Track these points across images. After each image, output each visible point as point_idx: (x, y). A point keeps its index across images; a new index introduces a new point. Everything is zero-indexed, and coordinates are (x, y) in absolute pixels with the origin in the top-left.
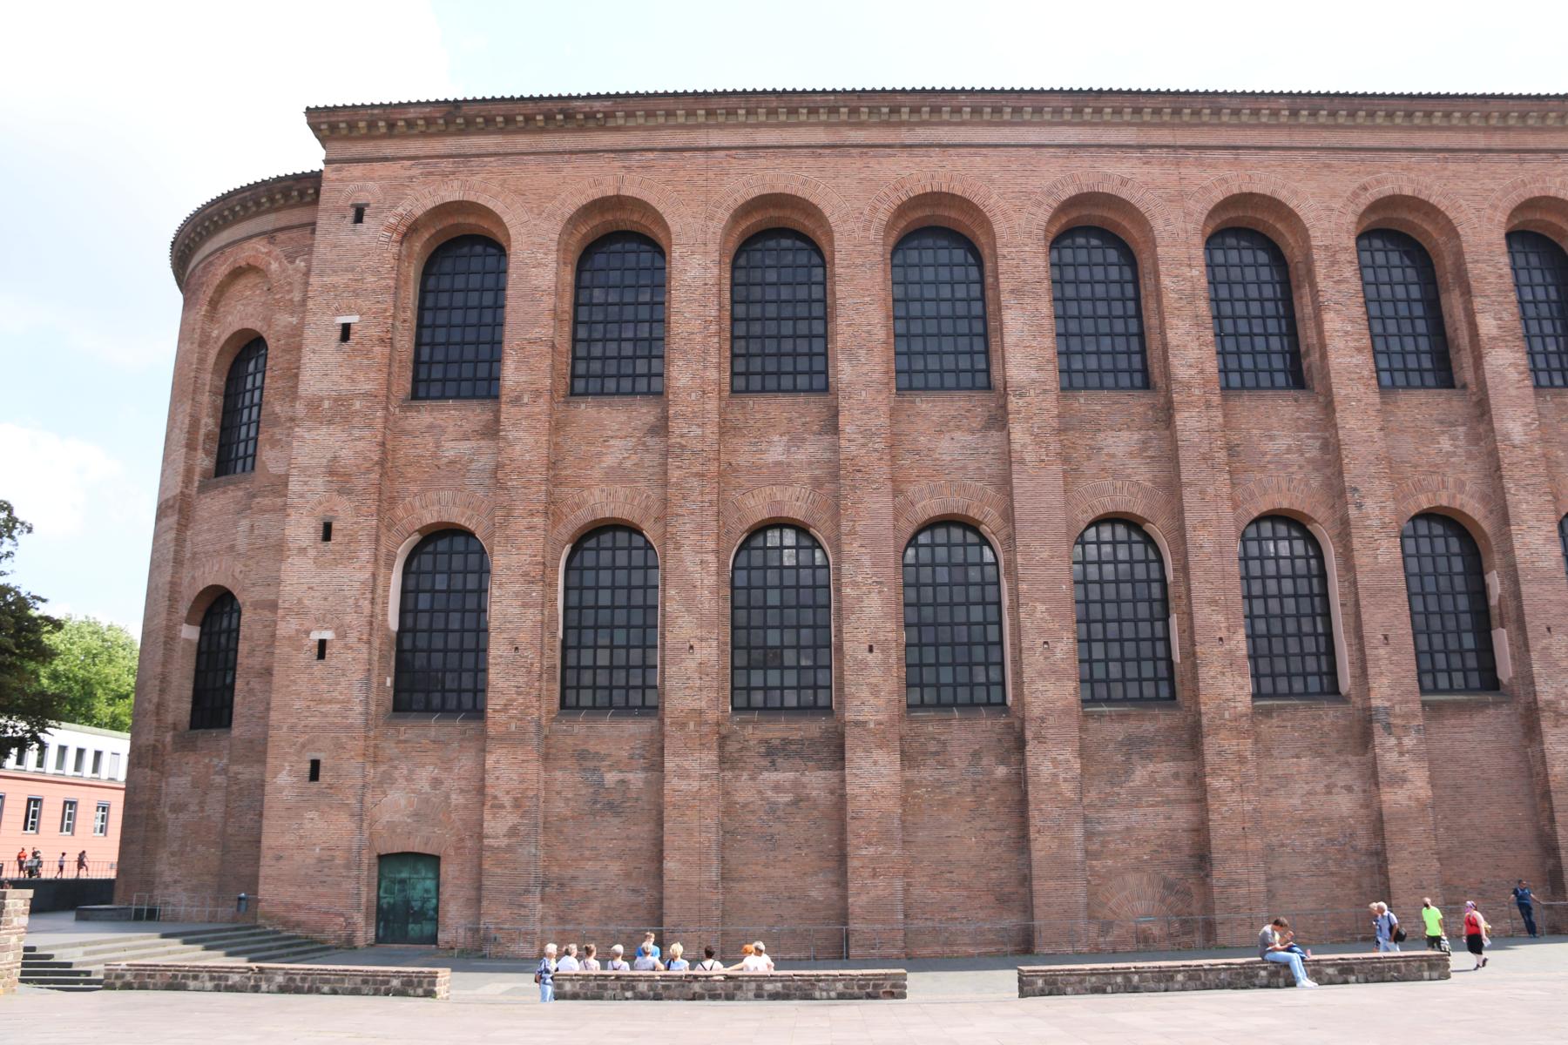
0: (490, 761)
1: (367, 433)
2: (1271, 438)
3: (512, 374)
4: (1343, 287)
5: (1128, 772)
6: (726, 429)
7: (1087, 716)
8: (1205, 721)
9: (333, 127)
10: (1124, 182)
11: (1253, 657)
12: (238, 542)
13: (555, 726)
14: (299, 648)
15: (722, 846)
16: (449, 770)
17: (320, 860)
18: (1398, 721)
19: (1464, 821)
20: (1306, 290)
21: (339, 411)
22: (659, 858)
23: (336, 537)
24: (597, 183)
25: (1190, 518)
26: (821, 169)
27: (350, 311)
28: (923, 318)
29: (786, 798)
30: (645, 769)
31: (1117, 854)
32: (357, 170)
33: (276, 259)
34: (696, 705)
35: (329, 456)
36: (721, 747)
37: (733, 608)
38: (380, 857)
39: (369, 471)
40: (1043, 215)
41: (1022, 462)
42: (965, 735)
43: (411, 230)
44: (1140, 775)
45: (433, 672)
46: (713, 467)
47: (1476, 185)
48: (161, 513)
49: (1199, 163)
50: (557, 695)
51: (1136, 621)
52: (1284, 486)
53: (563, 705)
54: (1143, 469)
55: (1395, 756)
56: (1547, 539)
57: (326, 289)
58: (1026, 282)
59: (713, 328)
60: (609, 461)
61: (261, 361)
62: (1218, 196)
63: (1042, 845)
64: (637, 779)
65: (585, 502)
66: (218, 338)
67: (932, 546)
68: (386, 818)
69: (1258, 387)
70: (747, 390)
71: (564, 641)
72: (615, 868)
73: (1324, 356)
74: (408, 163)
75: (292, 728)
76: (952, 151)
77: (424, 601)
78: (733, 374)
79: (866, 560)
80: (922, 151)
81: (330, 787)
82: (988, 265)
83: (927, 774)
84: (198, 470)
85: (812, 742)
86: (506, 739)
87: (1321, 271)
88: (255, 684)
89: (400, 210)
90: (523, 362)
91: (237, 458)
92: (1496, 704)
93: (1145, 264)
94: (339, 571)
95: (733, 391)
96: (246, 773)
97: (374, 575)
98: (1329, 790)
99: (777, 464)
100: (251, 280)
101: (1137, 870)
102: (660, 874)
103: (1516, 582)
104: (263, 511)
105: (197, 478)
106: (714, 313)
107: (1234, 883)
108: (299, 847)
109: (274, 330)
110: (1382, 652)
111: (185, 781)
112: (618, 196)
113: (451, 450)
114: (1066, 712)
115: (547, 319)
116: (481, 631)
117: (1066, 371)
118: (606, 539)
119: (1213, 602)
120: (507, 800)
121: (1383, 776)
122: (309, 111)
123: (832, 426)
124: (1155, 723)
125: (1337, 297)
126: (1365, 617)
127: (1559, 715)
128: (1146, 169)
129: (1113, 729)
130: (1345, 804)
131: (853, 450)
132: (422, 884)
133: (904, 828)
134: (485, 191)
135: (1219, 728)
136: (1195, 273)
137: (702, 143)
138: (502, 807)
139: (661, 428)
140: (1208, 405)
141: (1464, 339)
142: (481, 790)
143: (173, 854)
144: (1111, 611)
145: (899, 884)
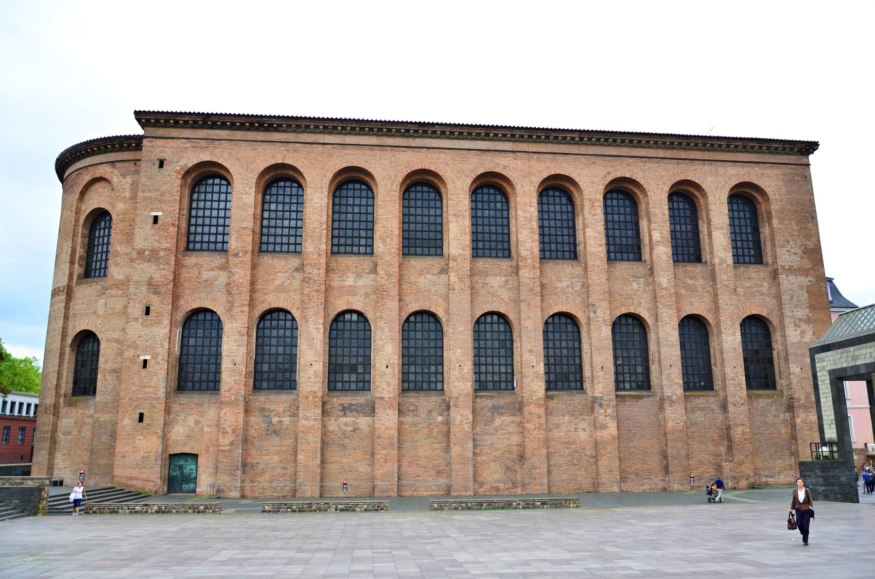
0: (222, 414)
1: (166, 266)
2: (560, 281)
3: (234, 243)
4: (596, 217)
5: (493, 420)
6: (328, 270)
7: (476, 397)
8: (525, 400)
9: (148, 121)
10: (505, 167)
11: (547, 373)
13: (251, 397)
14: (134, 363)
15: (322, 449)
17: (143, 457)
18: (605, 403)
19: (631, 444)
20: (580, 217)
21: (153, 256)
22: (296, 453)
23: (152, 313)
24: (274, 157)
25: (523, 315)
26: (374, 156)
27: (158, 210)
28: (416, 223)
29: (350, 429)
30: (290, 416)
31: (487, 454)
32: (160, 142)
33: (116, 175)
34: (313, 389)
35: (148, 276)
36: (323, 407)
37: (330, 347)
38: (170, 455)
39: (167, 284)
40: (469, 181)
41: (454, 289)
42: (425, 402)
43: (188, 172)
44: (498, 421)
45: (195, 372)
46: (323, 287)
47: (657, 174)
48: (55, 293)
49: (539, 159)
50: (252, 384)
51: (499, 357)
52: (564, 302)
53: (255, 388)
54: (505, 293)
55: (603, 417)
56: (673, 328)
57: (145, 199)
58: (460, 211)
59: (325, 226)
60: (277, 282)
61: (108, 223)
62: (545, 175)
63: (455, 450)
64: (286, 420)
65: (266, 300)
67: (415, 322)
68: (174, 438)
69: (557, 258)
70: (338, 253)
71: (255, 360)
72: (276, 458)
73: (585, 247)
75: (130, 399)
76: (431, 150)
77: (192, 341)
78: (332, 245)
79: (387, 329)
80: (418, 150)
81: (149, 425)
82: (445, 202)
83: (409, 419)
84: (76, 274)
85: (362, 405)
86: (229, 403)
87: (586, 210)
88: (108, 377)
90: (239, 237)
91: (96, 269)
92: (648, 396)
93: (512, 204)
94: (153, 329)
95: (332, 253)
96: (104, 417)
97: (170, 331)
98: (576, 430)
99: (351, 286)
100: (102, 184)
101: (495, 461)
102: (295, 461)
103: (659, 346)
105: (75, 277)
106: (325, 219)
107: (535, 468)
108: (134, 452)
109: (117, 209)
110: (600, 374)
111: (70, 421)
112: (283, 164)
113: (206, 275)
114: (468, 395)
115: (251, 218)
116: (218, 355)
117: (475, 249)
118: (275, 315)
119: (531, 351)
120: (229, 430)
121: (598, 425)
122: (137, 113)
123: (374, 270)
124: (504, 399)
125: (593, 222)
126: (594, 359)
127: (672, 401)
128: (515, 161)
129: (487, 402)
130: (583, 435)
131: (383, 282)
132: (189, 467)
133: (399, 442)
134: (222, 157)
135: (530, 403)
136: (533, 209)
137: (322, 142)
138: (227, 433)
139: (301, 269)
140: (534, 268)
141: (646, 240)
142: (218, 425)
143: (64, 455)
144: (489, 352)
145: (396, 466)
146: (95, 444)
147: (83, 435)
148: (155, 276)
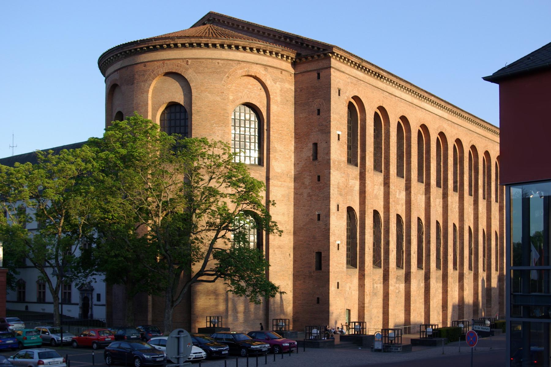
74: (348, 76)
88: (276, 251)
104: (275, 186)
120: (368, 293)
148: (340, 181)
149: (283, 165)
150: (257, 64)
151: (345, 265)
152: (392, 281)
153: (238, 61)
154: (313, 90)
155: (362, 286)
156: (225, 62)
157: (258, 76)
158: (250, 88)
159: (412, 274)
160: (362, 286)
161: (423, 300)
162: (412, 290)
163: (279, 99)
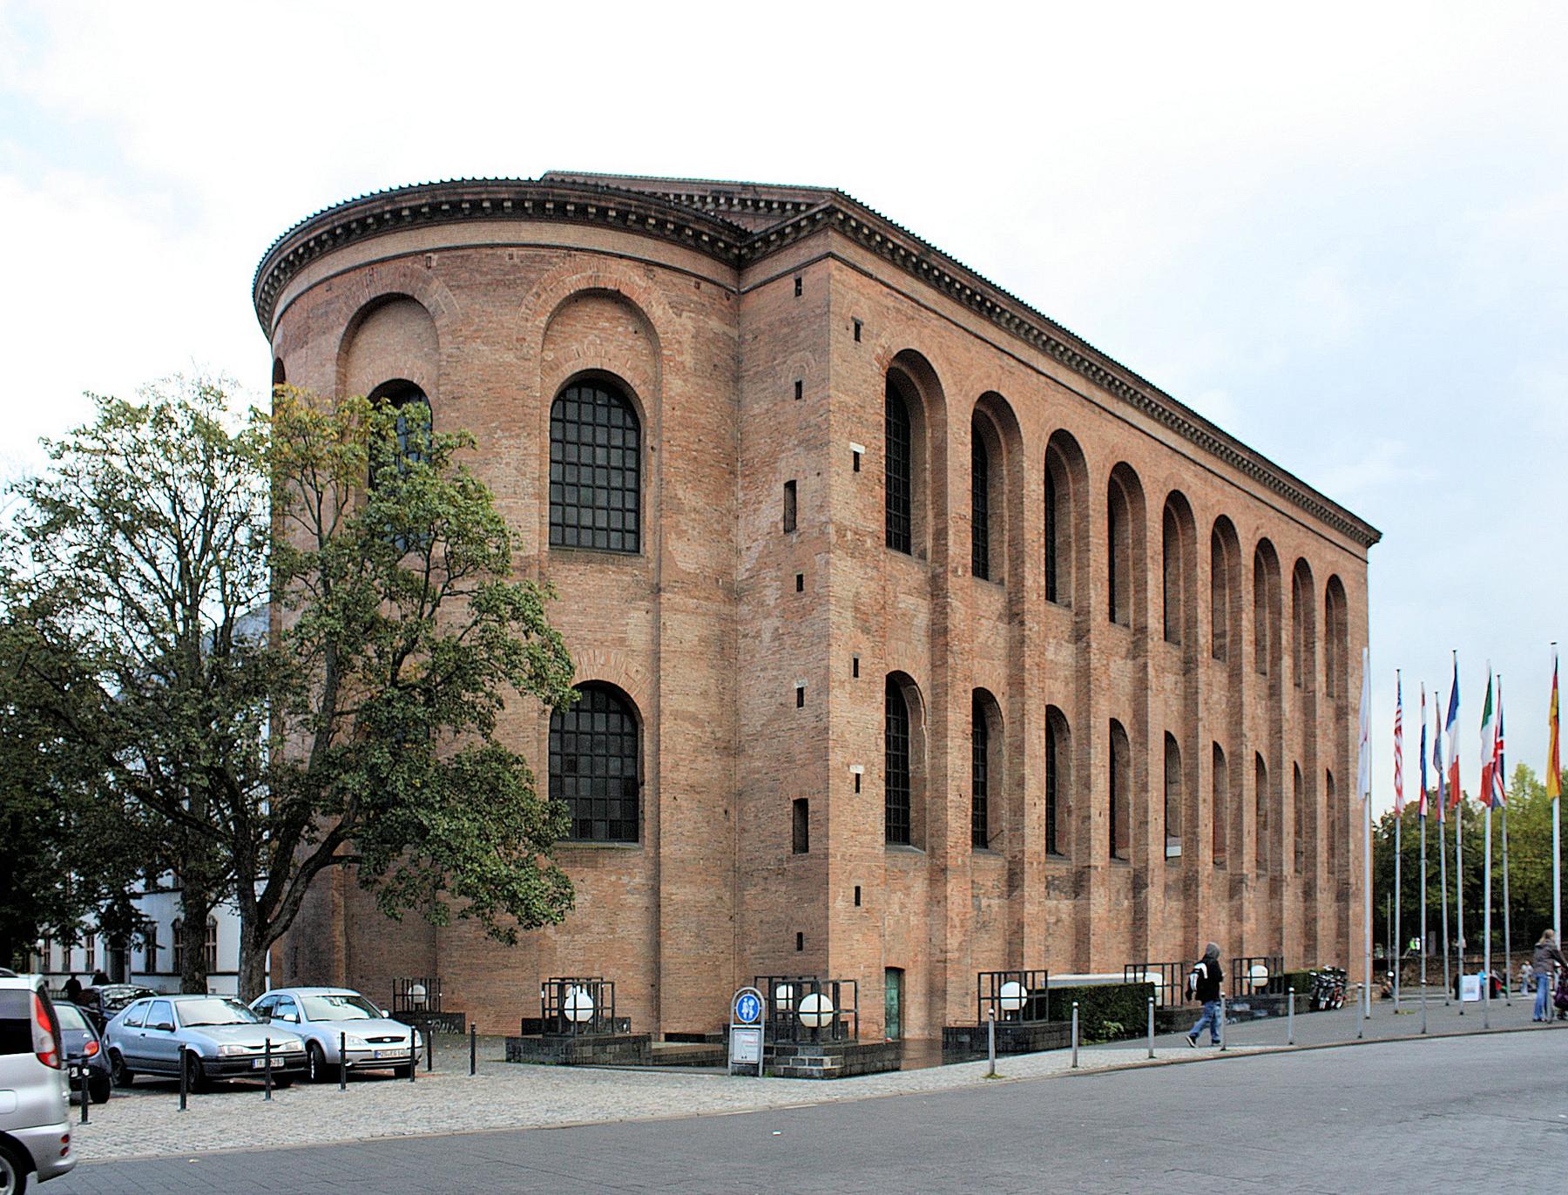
12: (631, 635)
16: (908, 895)
66: (555, 366)
74: (886, 290)
88: (682, 800)
89: (883, 341)
100: (610, 310)
146: (666, 952)
147: (620, 933)
149: (702, 551)
150: (621, 257)
151: (882, 840)
152: (1033, 888)
153: (569, 249)
154: (786, 330)
155: (936, 900)
156: (531, 252)
157: (625, 291)
158: (603, 329)
159: (1093, 871)
160: (936, 900)
161: (1128, 945)
162: (1093, 915)
163: (688, 359)
